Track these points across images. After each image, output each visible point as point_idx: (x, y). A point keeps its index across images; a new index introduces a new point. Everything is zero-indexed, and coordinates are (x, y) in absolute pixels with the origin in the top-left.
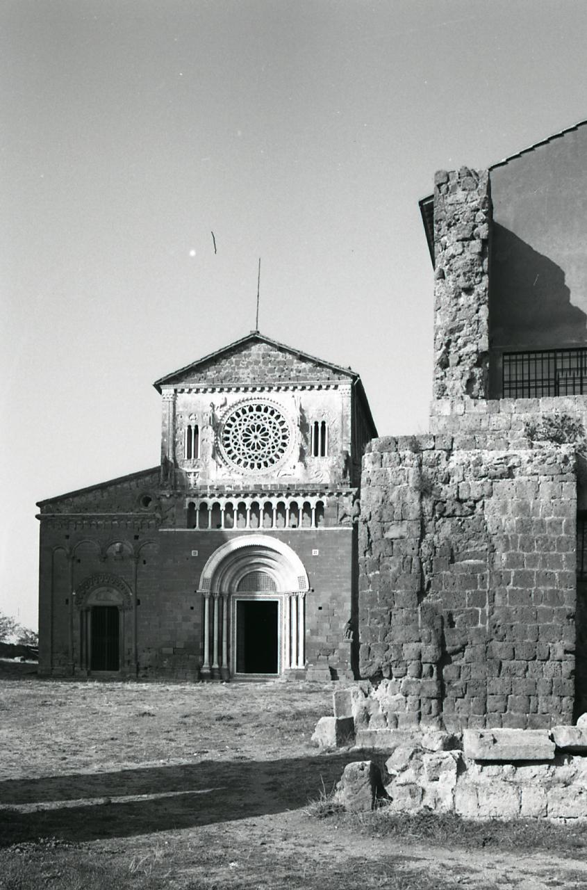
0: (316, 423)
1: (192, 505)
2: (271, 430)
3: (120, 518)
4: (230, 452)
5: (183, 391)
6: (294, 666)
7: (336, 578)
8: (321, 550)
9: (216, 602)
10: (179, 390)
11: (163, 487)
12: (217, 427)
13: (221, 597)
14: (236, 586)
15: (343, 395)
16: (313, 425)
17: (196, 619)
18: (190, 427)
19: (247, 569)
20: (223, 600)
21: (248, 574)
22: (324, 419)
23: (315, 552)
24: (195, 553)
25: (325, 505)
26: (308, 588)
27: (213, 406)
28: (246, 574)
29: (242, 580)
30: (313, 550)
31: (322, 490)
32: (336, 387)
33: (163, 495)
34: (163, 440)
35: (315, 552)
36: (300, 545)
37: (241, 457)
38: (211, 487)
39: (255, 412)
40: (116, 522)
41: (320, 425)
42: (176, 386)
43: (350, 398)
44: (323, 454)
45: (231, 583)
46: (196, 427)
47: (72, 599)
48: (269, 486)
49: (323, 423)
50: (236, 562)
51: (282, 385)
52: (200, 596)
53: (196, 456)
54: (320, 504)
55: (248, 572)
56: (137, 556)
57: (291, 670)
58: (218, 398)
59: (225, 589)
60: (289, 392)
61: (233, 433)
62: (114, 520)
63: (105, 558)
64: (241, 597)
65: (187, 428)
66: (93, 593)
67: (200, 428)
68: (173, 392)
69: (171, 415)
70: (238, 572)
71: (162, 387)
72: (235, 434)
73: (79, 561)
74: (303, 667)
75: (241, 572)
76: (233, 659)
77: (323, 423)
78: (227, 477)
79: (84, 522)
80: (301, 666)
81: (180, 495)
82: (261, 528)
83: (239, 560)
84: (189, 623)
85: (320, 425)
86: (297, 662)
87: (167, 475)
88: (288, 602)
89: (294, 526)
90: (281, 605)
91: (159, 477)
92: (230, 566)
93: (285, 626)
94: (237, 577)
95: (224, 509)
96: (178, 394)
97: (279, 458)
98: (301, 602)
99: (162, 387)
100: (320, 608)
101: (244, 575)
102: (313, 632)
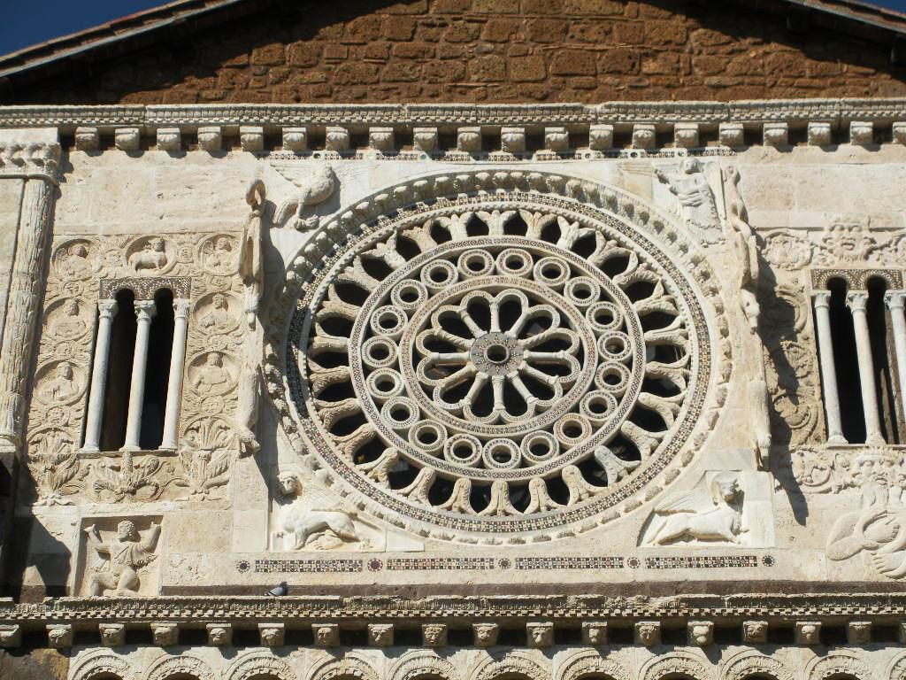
5: (105, 141)
10: (86, 133)
12: (282, 317)
16: (824, 295)
22: (874, 265)
27: (265, 212)
41: (857, 303)
42: (66, 112)
46: (164, 299)
49: (877, 287)
53: (151, 437)
58: (293, 178)
60: (675, 159)
61: (369, 333)
65: (111, 302)
67: (181, 304)
68: (50, 136)
69: (29, 234)
72: (383, 336)
77: (877, 287)
85: (857, 303)
96: (76, 156)
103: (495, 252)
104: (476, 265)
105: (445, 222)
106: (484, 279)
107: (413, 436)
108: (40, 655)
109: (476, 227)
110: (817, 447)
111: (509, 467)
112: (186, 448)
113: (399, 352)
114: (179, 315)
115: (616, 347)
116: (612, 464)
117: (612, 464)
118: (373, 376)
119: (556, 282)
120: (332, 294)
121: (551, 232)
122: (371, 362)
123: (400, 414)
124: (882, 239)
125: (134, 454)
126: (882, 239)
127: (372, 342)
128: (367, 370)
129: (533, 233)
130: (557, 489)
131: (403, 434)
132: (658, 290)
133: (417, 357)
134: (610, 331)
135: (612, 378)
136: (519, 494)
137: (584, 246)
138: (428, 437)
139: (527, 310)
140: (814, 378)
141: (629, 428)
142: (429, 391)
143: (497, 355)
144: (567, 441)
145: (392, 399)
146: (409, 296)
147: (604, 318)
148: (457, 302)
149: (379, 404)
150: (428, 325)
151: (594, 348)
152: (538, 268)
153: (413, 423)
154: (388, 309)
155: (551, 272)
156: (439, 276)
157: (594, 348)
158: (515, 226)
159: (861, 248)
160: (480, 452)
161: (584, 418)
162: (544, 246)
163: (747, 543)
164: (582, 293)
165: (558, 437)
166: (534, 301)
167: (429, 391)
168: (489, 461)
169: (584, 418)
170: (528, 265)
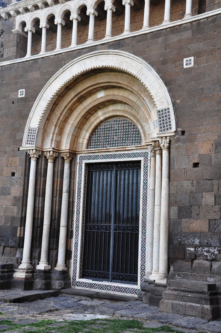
8: (197, 55)
14: (85, 142)
17: (16, 191)
21: (101, 122)
23: (189, 62)
24: (21, 93)
26: (174, 129)
28: (98, 121)
52: (23, 157)
55: (102, 118)
59: (65, 146)
64: (90, 158)
75: (92, 119)
76: (76, 256)
82: (108, 38)
84: (8, 196)
90: (146, 167)
100: (196, 165)
101: (95, 124)
108: (11, 20)
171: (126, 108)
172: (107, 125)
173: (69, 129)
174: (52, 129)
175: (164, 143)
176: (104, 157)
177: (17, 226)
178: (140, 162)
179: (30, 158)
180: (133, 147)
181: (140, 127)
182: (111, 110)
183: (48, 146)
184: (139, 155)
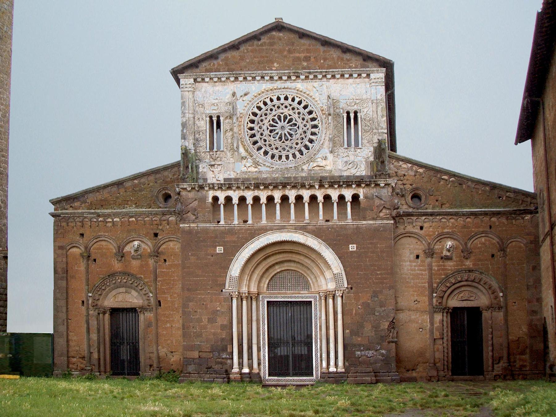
0: (348, 113)
1: (216, 199)
2: (300, 121)
3: (136, 215)
4: (255, 143)
6: (332, 369)
7: (378, 274)
9: (244, 302)
11: (184, 180)
13: (250, 297)
15: (377, 84)
16: (345, 115)
18: (211, 117)
19: (277, 267)
20: (251, 299)
21: (278, 273)
22: (355, 108)
23: (353, 247)
25: (362, 197)
28: (276, 272)
29: (272, 278)
30: (350, 246)
31: (359, 182)
32: (368, 76)
33: (182, 189)
34: (182, 131)
35: (353, 247)
36: (336, 239)
37: (268, 149)
38: (236, 179)
39: (282, 100)
40: (134, 219)
41: (352, 115)
43: (384, 87)
44: (357, 145)
45: (260, 282)
46: (218, 117)
47: (88, 300)
48: (300, 178)
49: (356, 113)
50: (265, 259)
51: (310, 73)
54: (355, 197)
55: (279, 270)
56: (156, 254)
57: (329, 373)
61: (258, 123)
62: (132, 217)
63: (122, 257)
65: (208, 119)
66: (110, 294)
68: (192, 81)
70: (267, 270)
71: (180, 76)
73: (95, 260)
74: (343, 370)
77: (356, 113)
78: (253, 169)
79: (100, 219)
80: (341, 369)
81: (201, 187)
83: (269, 257)
85: (352, 115)
86: (336, 365)
87: (187, 167)
88: (323, 301)
89: (327, 221)
90: (316, 305)
91: (179, 171)
92: (258, 265)
93: (321, 326)
94: (266, 276)
95: (251, 203)
97: (302, 154)
98: (339, 301)
99: (180, 76)
101: (273, 274)
102: (352, 333)
103: (282, 104)
104: (278, 107)
105: (272, 97)
106: (281, 111)
107: (267, 145)
108: (204, 192)
109: (278, 99)
110: (342, 148)
111: (285, 152)
112: (225, 150)
113: (264, 127)
114: (222, 121)
115: (305, 126)
116: (305, 151)
117: (305, 151)
118: (260, 133)
119: (294, 111)
120: (251, 114)
121: (293, 100)
122: (259, 130)
123: (265, 141)
124: (358, 101)
125: (216, 152)
126: (358, 101)
127: (259, 125)
128: (259, 132)
129: (290, 99)
130: (294, 156)
131: (265, 145)
132: (314, 113)
133: (268, 129)
134: (305, 122)
135: (305, 132)
136: (287, 157)
137: (300, 103)
138: (270, 145)
139: (289, 118)
140: (342, 133)
141: (308, 143)
142: (270, 136)
143: (283, 128)
144: (296, 146)
145: (264, 137)
146: (266, 115)
147: (303, 119)
148: (275, 116)
149: (261, 139)
150: (269, 121)
151: (301, 126)
152: (291, 108)
153: (267, 143)
154: (262, 118)
155: (293, 109)
156: (271, 110)
157: (301, 126)
158: (286, 98)
159: (353, 104)
160: (280, 149)
161: (299, 141)
162: (292, 103)
163: (328, 168)
164: (299, 113)
165: (294, 145)
166: (290, 115)
167: (270, 136)
168: (282, 151)
169: (299, 141)
170: (289, 107)
171: (299, 266)
172: (282, 275)
173: (256, 277)
174: (246, 277)
175: (338, 294)
176: (283, 297)
177: (226, 344)
178: (311, 302)
179: (232, 298)
180: (306, 292)
181: (309, 279)
182: (285, 266)
183: (244, 289)
184: (310, 297)
